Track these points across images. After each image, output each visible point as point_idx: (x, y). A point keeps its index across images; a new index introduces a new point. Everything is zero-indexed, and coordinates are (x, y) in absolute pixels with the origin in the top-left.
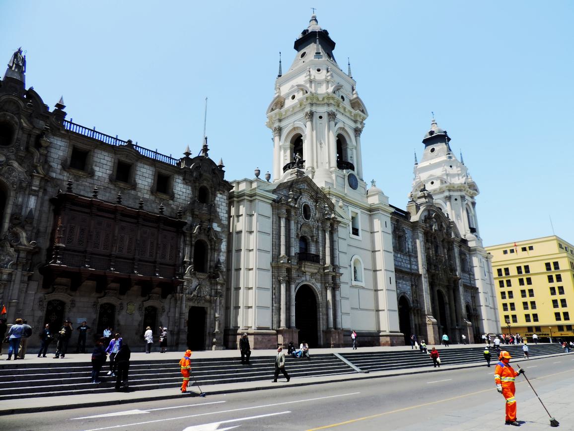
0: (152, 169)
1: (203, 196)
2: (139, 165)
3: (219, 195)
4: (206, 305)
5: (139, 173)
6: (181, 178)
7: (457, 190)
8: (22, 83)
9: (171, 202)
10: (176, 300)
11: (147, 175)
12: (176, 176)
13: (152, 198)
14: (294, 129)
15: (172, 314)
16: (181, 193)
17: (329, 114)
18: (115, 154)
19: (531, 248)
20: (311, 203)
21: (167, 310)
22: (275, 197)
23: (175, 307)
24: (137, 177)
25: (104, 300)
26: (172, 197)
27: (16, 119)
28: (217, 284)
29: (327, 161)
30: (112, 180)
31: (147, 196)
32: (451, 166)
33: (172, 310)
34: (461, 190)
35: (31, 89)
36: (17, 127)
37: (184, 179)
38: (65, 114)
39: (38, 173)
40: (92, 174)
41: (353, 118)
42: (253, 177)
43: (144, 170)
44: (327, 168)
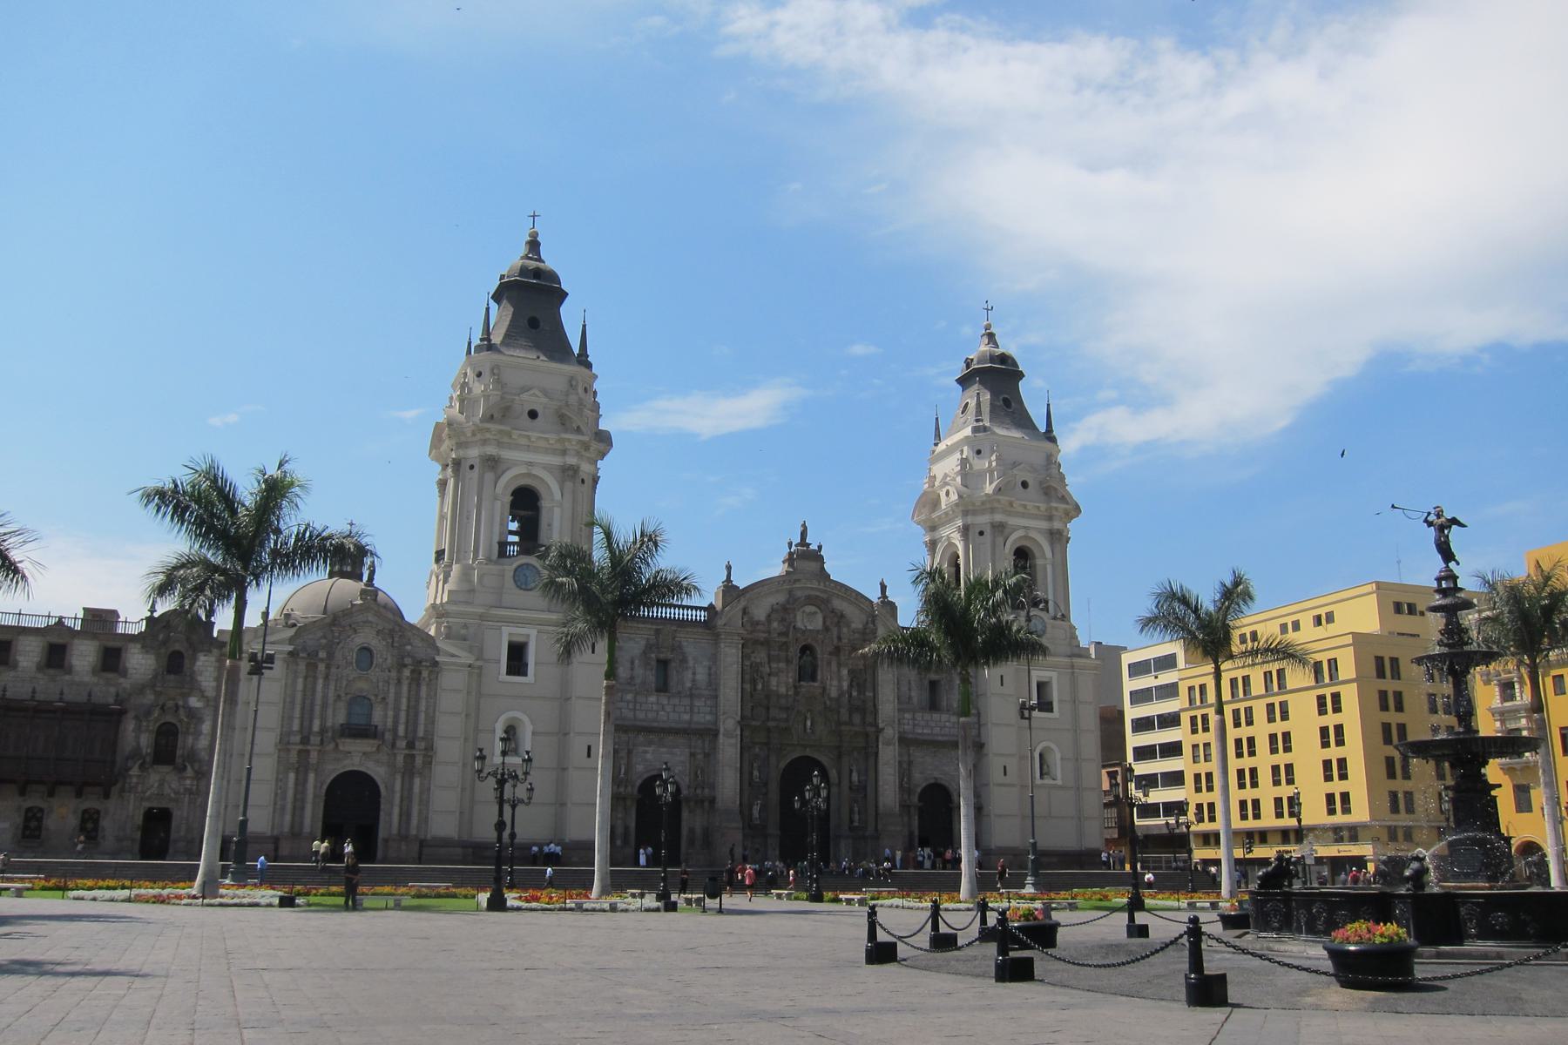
1: (175, 664)
2: (76, 641)
4: (170, 806)
7: (983, 512)
9: (121, 680)
12: (131, 645)
13: (95, 679)
19: (1330, 618)
20: (375, 643)
22: (291, 648)
25: (29, 804)
26: (124, 674)
28: (185, 778)
30: (39, 668)
31: (86, 679)
32: (979, 452)
34: (993, 510)
40: (15, 666)
43: (83, 648)
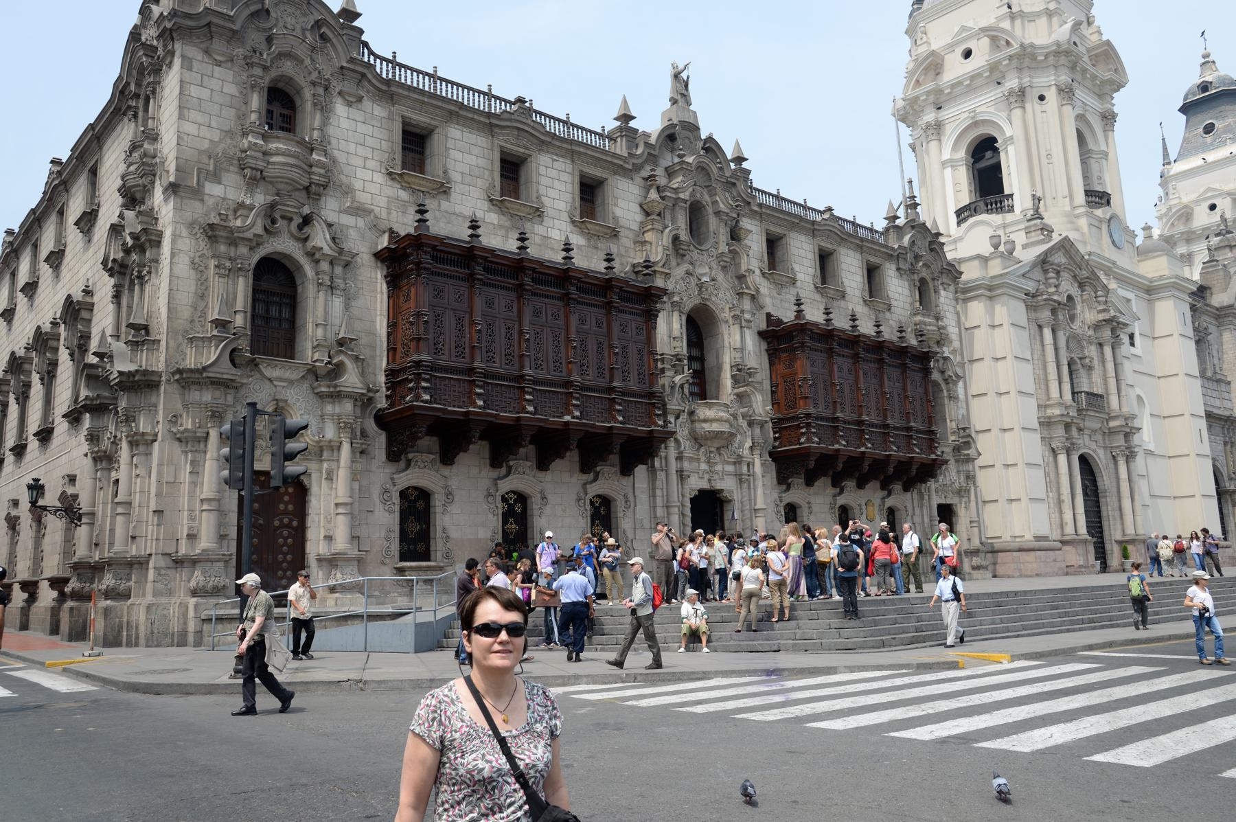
0: (858, 256)
3: (942, 292)
5: (844, 266)
6: (894, 267)
8: (695, 128)
10: (920, 493)
11: (853, 269)
14: (976, 124)
15: (917, 519)
16: (896, 296)
17: (1060, 90)
18: (814, 236)
21: (910, 512)
23: (921, 507)
24: (844, 274)
25: (841, 500)
27: (707, 197)
29: (1066, 193)
33: (917, 511)
35: (710, 139)
36: (710, 210)
37: (898, 269)
38: (748, 172)
39: (748, 288)
41: (1097, 90)
42: (987, 250)
44: (1068, 208)
